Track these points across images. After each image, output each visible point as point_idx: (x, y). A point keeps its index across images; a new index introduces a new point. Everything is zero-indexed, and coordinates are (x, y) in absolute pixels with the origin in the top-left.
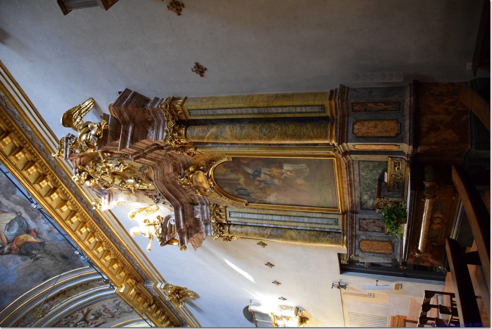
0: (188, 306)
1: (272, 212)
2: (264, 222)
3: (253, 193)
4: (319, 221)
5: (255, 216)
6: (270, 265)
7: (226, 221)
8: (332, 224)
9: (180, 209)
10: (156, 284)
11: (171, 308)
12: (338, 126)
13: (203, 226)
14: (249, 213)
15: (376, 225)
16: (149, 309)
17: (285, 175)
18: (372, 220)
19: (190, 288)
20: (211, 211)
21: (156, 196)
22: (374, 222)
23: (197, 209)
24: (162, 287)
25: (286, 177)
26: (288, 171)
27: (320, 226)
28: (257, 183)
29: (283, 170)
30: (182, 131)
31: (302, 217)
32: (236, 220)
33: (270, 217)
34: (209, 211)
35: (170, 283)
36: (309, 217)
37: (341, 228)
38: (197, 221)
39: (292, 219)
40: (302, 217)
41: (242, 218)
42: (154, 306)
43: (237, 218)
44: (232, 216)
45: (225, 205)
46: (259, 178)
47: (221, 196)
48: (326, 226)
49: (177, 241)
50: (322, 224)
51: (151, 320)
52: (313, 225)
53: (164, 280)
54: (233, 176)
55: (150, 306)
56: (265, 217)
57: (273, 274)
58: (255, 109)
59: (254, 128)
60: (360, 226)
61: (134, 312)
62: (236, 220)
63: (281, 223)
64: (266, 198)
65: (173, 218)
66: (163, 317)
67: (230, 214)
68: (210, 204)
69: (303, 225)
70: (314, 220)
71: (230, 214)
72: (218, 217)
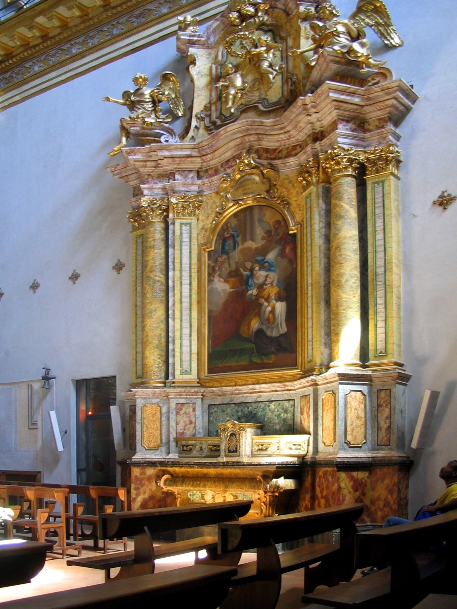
3: (229, 259)
4: (186, 349)
14: (190, 252)
15: (186, 425)
17: (266, 304)
18: (193, 420)
21: (210, 116)
22: (191, 422)
25: (261, 305)
28: (249, 265)
29: (274, 302)
30: (350, 171)
31: (191, 326)
39: (186, 312)
46: (257, 268)
50: (181, 353)
52: (177, 342)
54: (259, 232)
58: (383, 269)
60: (183, 404)
64: (220, 276)
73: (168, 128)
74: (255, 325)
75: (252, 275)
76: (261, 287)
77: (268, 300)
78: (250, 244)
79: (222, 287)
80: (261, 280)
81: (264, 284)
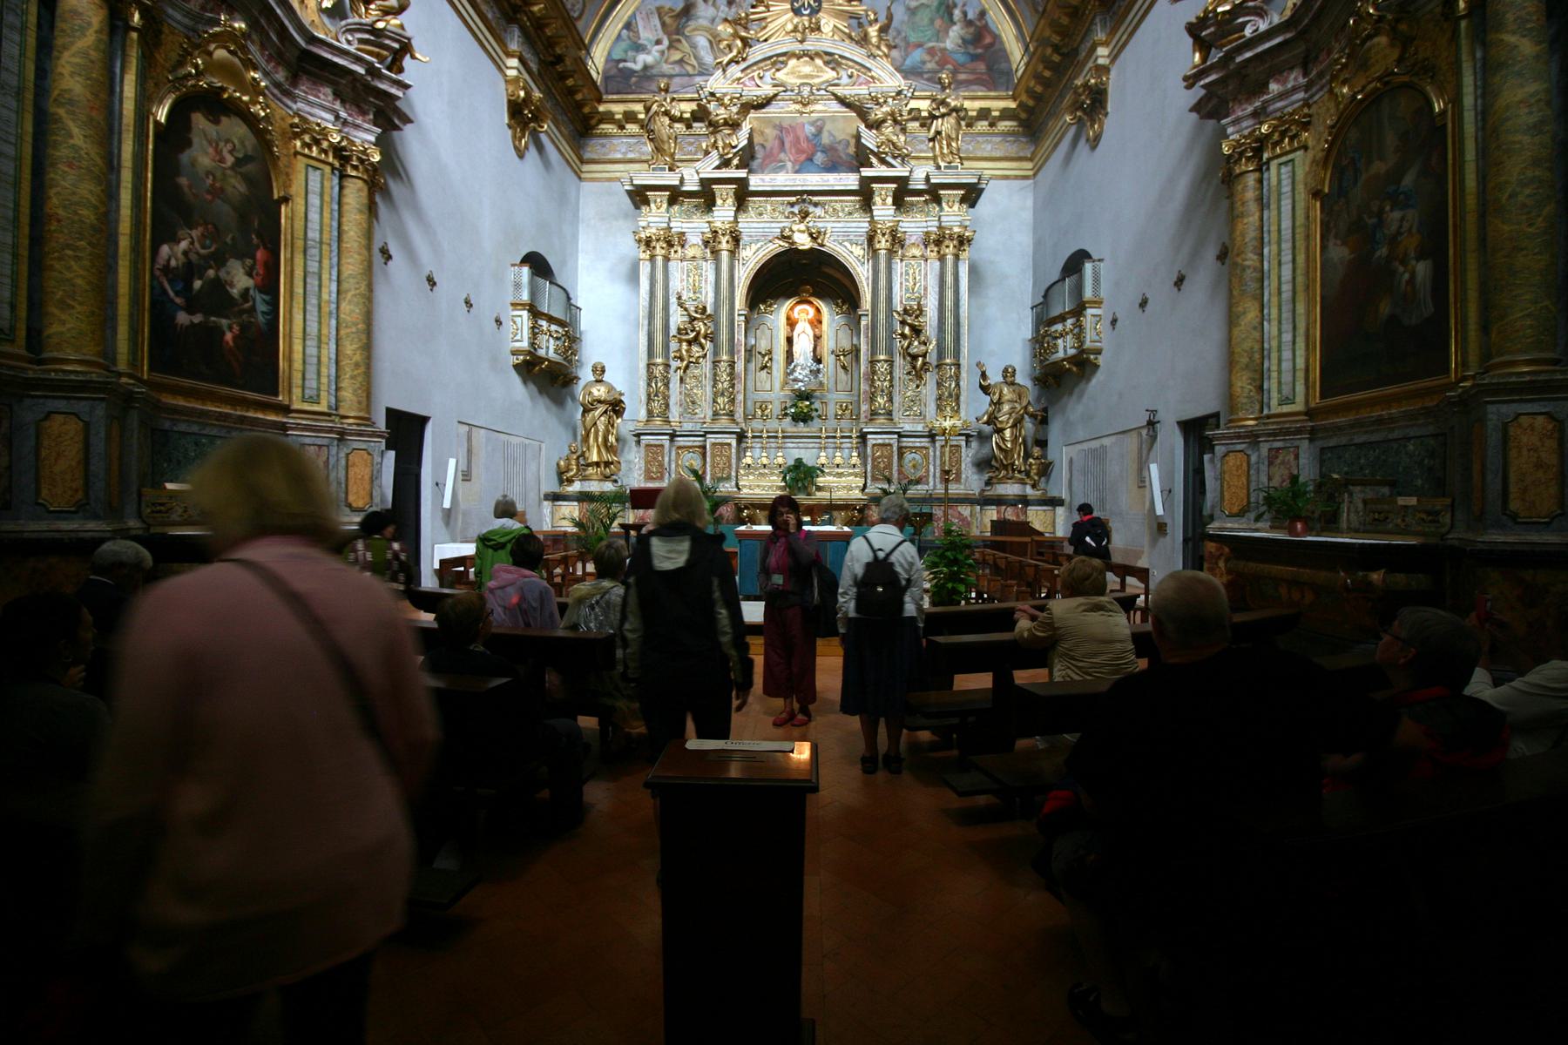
0: (1073, 130)
1: (1301, 259)
2: (1274, 247)
4: (1286, 365)
5: (1286, 224)
6: (1179, 282)
7: (1269, 160)
8: (1280, 392)
9: (1288, 35)
10: (1105, 44)
11: (1062, 96)
12: (1542, 377)
13: (1250, 109)
16: (1049, 51)
17: (1401, 269)
19: (1109, 123)
20: (1291, 114)
23: (1295, 78)
24: (1101, 61)
26: (1413, 274)
27: (1274, 368)
29: (1413, 262)
31: (1294, 328)
32: (1274, 181)
33: (1287, 257)
34: (1290, 109)
35: (1113, 74)
36: (1294, 342)
37: (1273, 411)
38: (1262, 87)
39: (1286, 308)
40: (1294, 328)
41: (1280, 194)
42: (1056, 58)
43: (1279, 181)
44: (1284, 170)
45: (1310, 143)
47: (1332, 127)
48: (1274, 383)
49: (1204, 59)
50: (1280, 372)
51: (1027, 65)
52: (1274, 355)
53: (1113, 61)
54: (1391, 140)
55: (1056, 48)
56: (1287, 246)
57: (1161, 292)
59: (1536, 162)
61: (1035, 19)
62: (1274, 181)
63: (1274, 284)
64: (1336, 237)
65: (1263, 26)
66: (1039, 89)
67: (1285, 163)
68: (1309, 106)
69: (1275, 331)
70: (1287, 354)
71: (1285, 163)
72: (1276, 137)
73: (1255, 8)
74: (1385, 308)
75: (1381, 222)
76: (1393, 241)
77: (1403, 262)
78: (1379, 167)
79: (1340, 253)
80: (1394, 228)
81: (1399, 233)
